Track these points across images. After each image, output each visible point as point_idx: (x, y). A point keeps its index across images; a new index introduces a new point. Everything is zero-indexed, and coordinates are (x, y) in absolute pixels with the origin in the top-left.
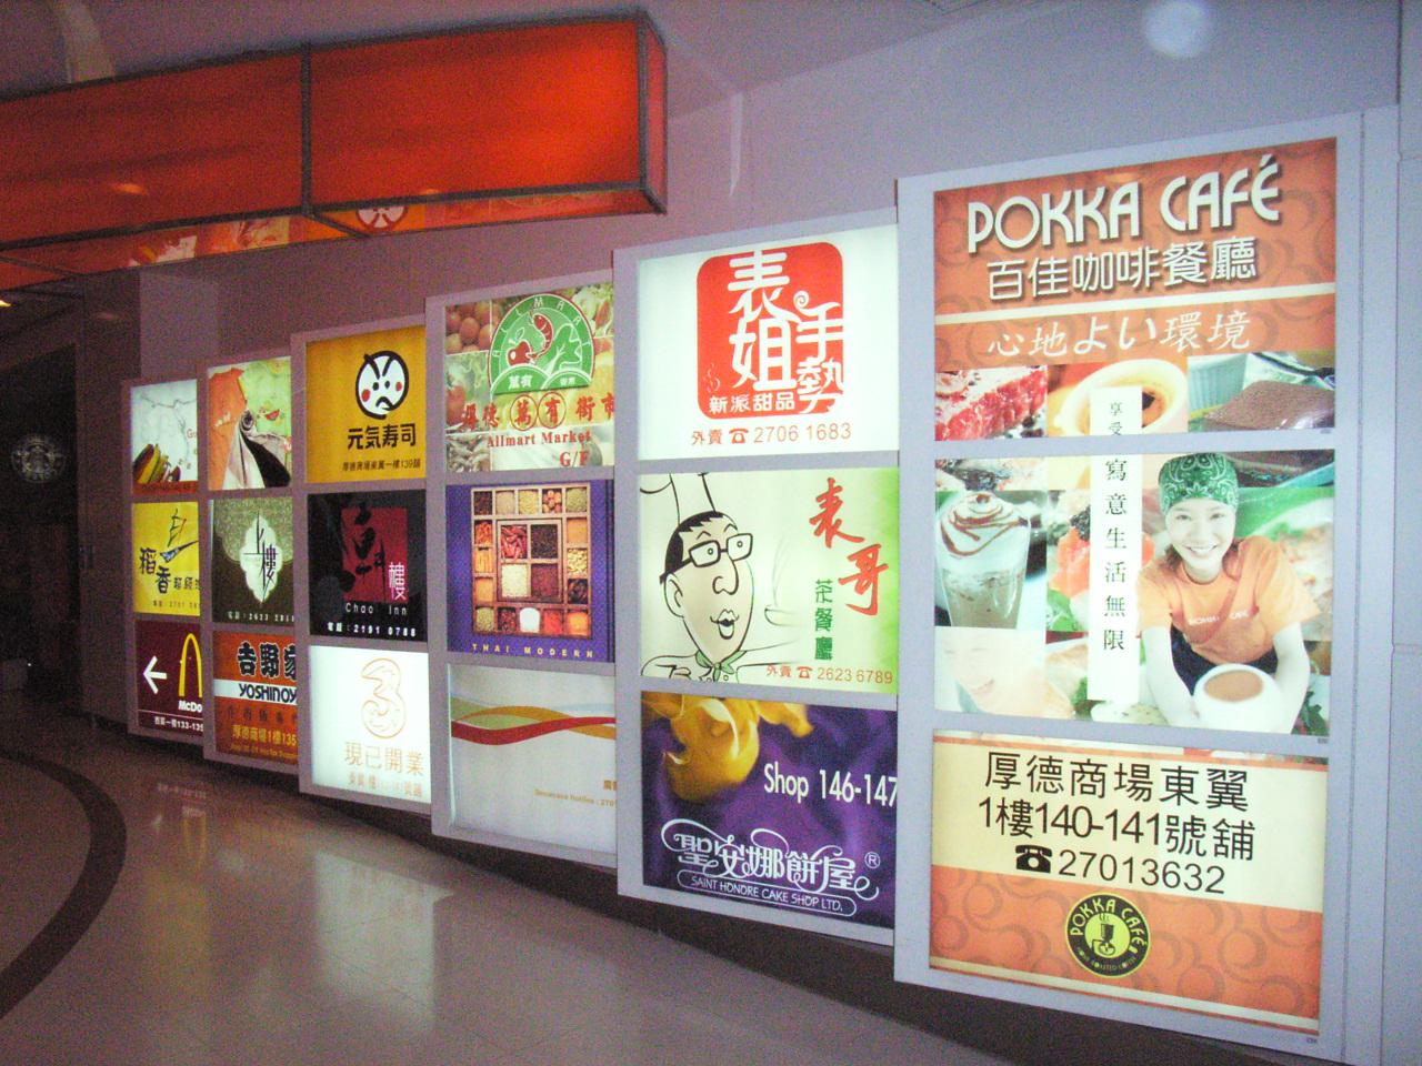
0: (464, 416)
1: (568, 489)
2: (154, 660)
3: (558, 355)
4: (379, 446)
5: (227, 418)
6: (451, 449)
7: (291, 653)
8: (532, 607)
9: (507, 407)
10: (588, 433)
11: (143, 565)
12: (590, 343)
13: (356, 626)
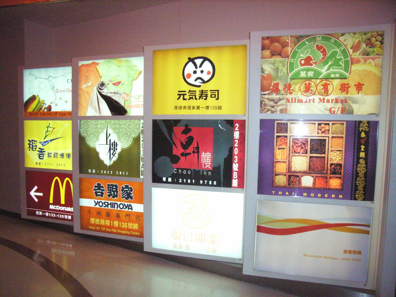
0: (271, 87)
1: (333, 124)
2: (36, 188)
3: (330, 63)
4: (196, 99)
5: (89, 84)
6: (263, 103)
7: (125, 188)
8: (309, 175)
9: (298, 85)
10: (346, 99)
11: (30, 147)
12: (349, 59)
13: (117, 172)
